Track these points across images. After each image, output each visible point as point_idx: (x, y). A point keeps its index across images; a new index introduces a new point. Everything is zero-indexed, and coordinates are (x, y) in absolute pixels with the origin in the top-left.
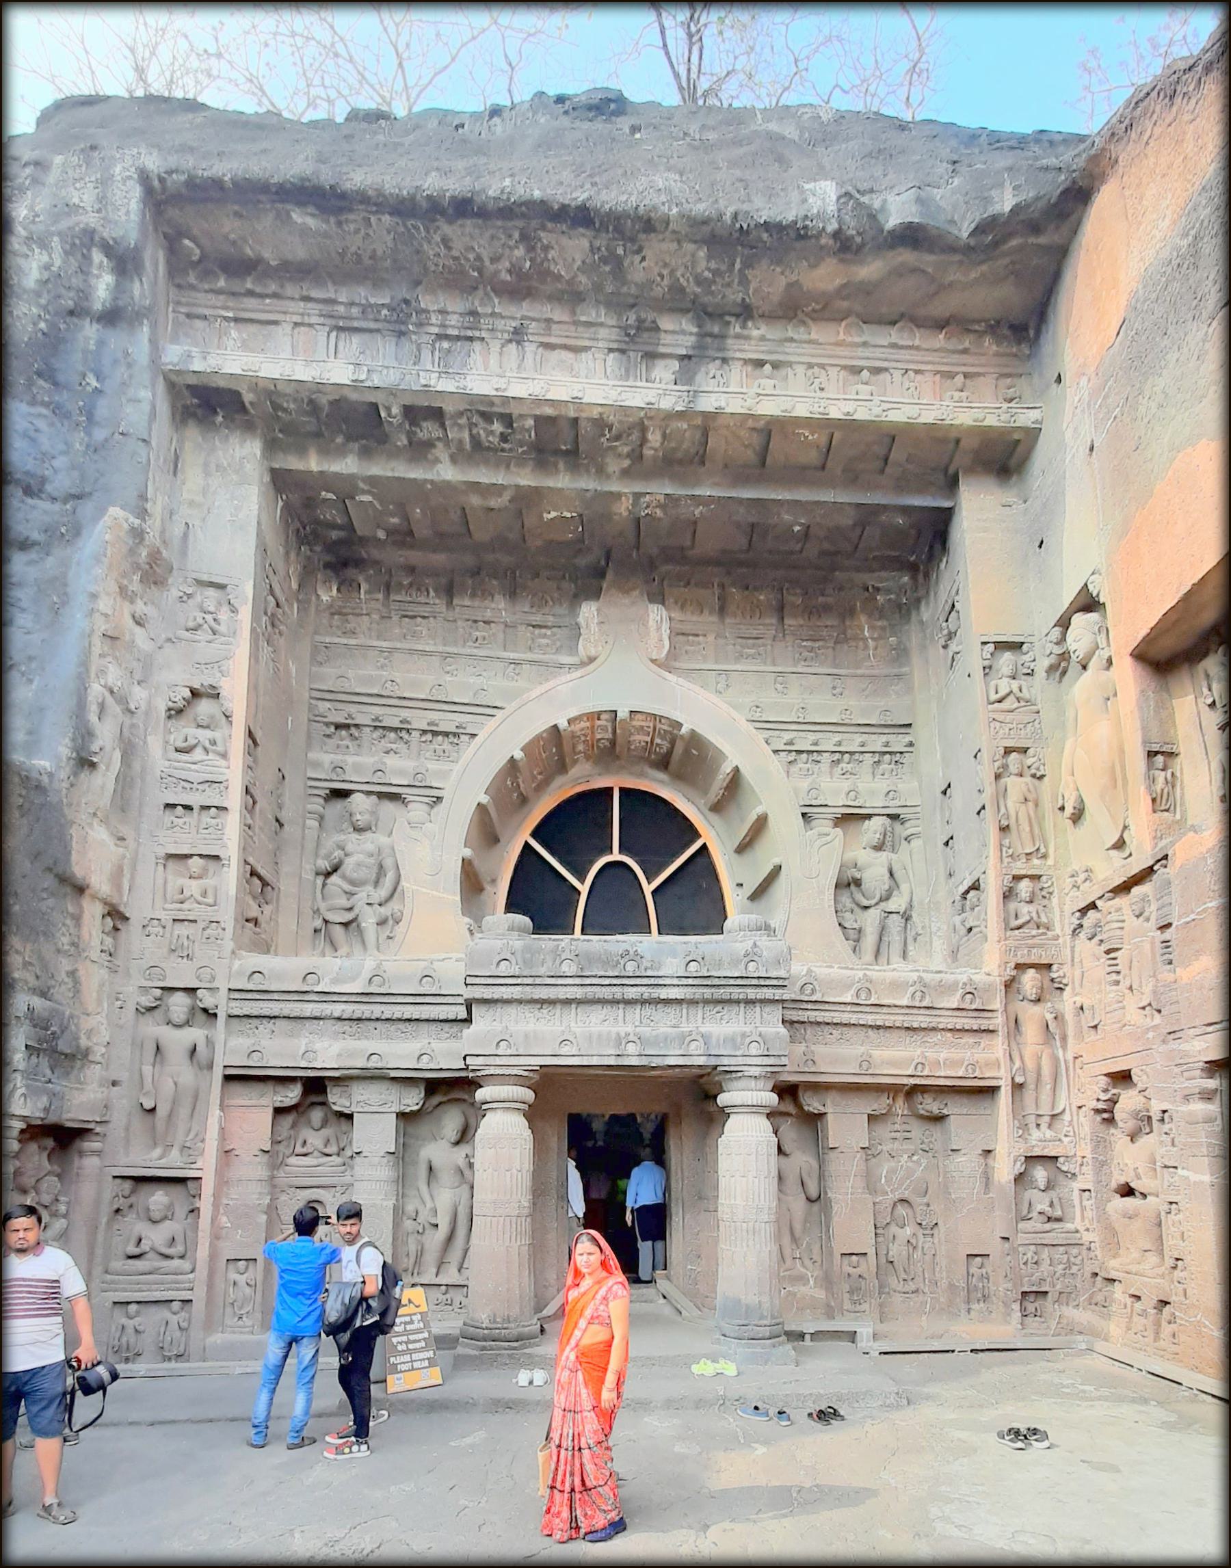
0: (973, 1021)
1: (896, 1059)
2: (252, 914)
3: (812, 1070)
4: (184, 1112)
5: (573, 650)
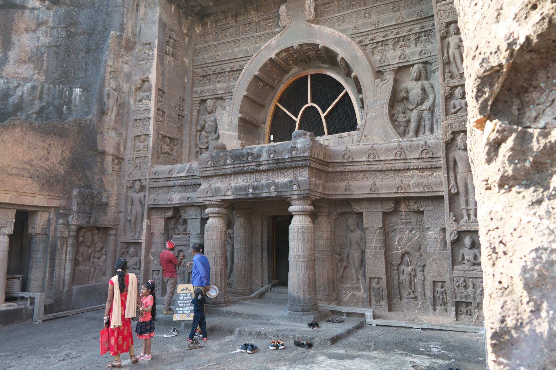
1: (387, 186)
2: (163, 151)
3: (349, 193)
5: (277, 26)
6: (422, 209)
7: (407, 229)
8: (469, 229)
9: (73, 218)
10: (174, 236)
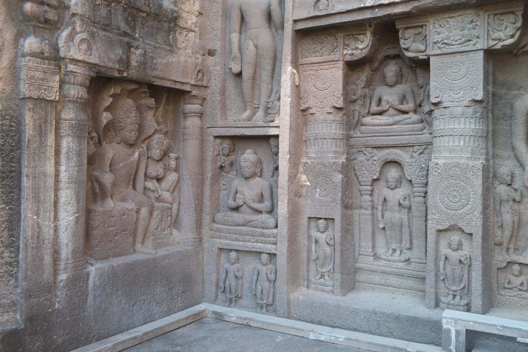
4: (265, 74)
9: (71, 37)
10: (368, 120)
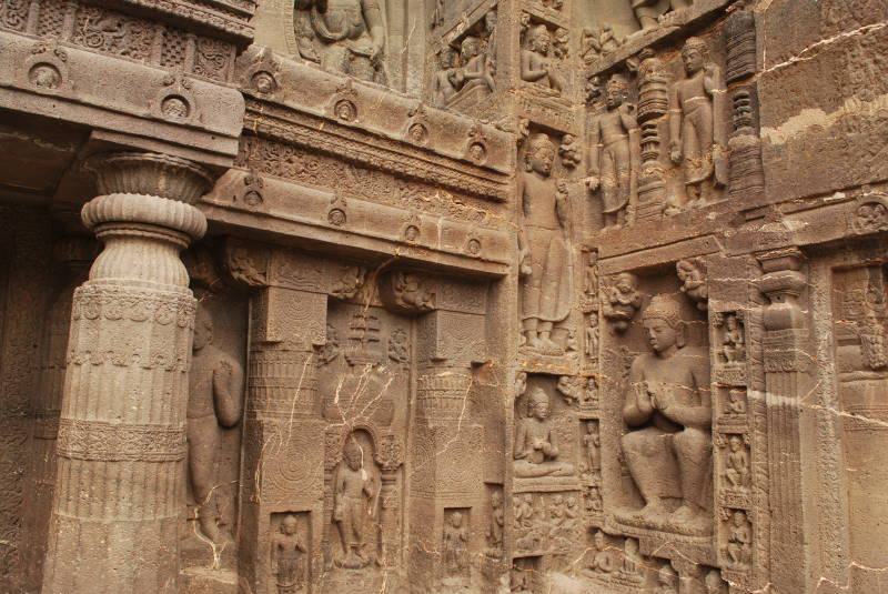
0: (480, 183)
1: (384, 217)
6: (430, 305)
7: (369, 359)
8: (549, 369)
